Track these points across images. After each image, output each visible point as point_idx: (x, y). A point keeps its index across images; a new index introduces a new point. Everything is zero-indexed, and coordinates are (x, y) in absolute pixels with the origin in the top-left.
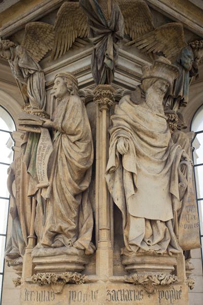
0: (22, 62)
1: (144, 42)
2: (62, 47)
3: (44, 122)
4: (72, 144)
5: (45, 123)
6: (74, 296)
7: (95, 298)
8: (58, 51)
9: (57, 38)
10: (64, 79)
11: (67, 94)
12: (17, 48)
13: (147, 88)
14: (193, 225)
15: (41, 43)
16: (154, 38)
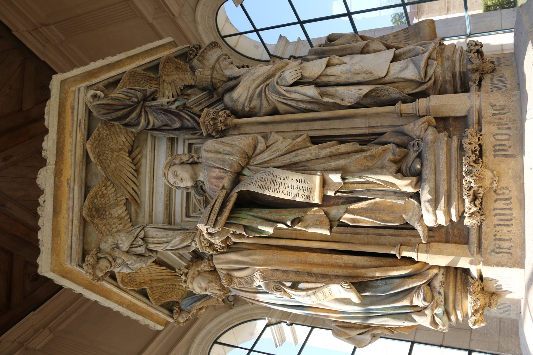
0: (124, 239)
1: (167, 93)
2: (130, 182)
3: (223, 188)
4: (268, 150)
5: (226, 187)
6: (501, 148)
7: (503, 109)
8: (132, 192)
9: (117, 182)
10: (174, 164)
11: (195, 167)
12: (102, 246)
13: (224, 76)
14: (405, 35)
15: (111, 211)
16: (167, 83)
